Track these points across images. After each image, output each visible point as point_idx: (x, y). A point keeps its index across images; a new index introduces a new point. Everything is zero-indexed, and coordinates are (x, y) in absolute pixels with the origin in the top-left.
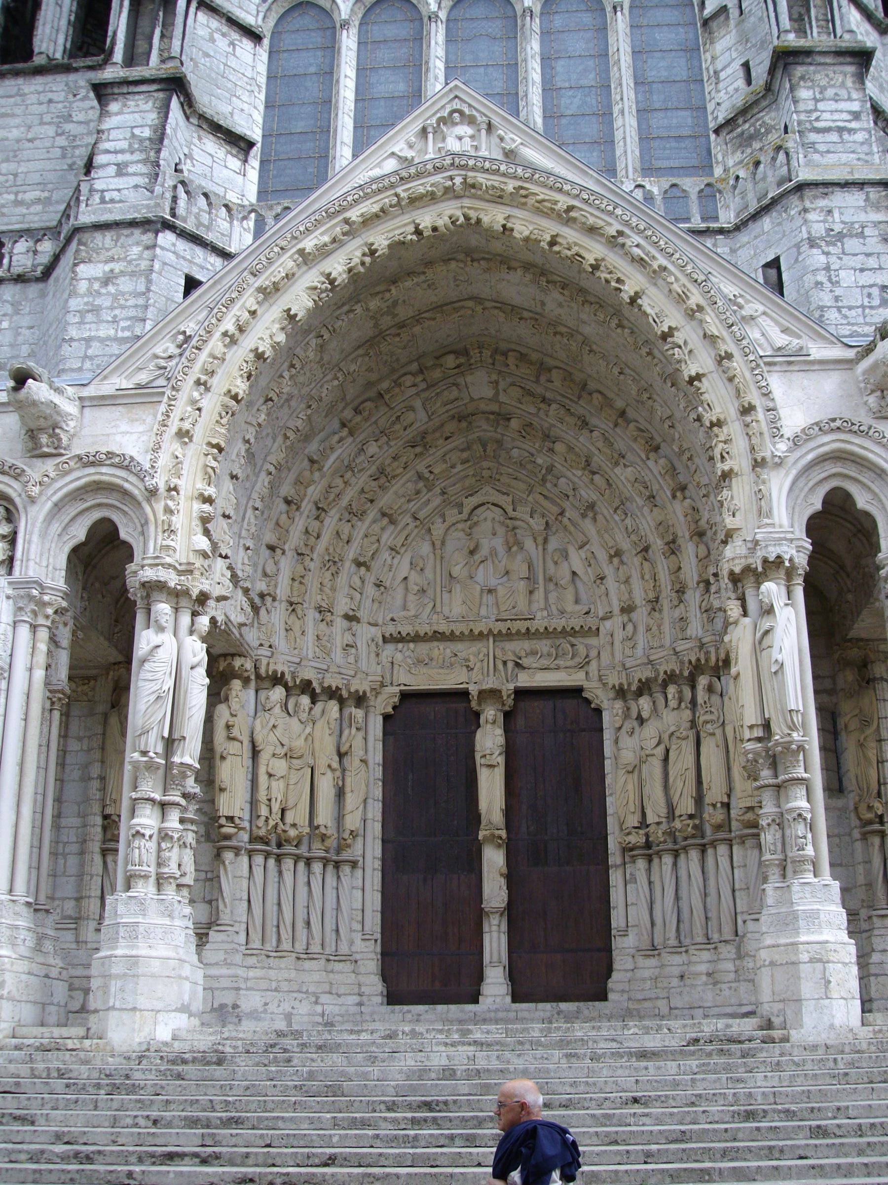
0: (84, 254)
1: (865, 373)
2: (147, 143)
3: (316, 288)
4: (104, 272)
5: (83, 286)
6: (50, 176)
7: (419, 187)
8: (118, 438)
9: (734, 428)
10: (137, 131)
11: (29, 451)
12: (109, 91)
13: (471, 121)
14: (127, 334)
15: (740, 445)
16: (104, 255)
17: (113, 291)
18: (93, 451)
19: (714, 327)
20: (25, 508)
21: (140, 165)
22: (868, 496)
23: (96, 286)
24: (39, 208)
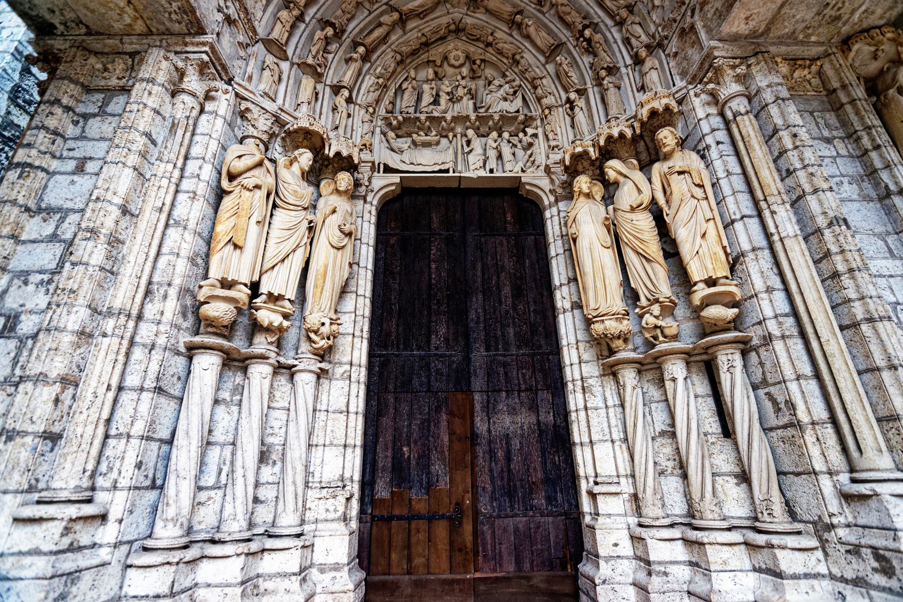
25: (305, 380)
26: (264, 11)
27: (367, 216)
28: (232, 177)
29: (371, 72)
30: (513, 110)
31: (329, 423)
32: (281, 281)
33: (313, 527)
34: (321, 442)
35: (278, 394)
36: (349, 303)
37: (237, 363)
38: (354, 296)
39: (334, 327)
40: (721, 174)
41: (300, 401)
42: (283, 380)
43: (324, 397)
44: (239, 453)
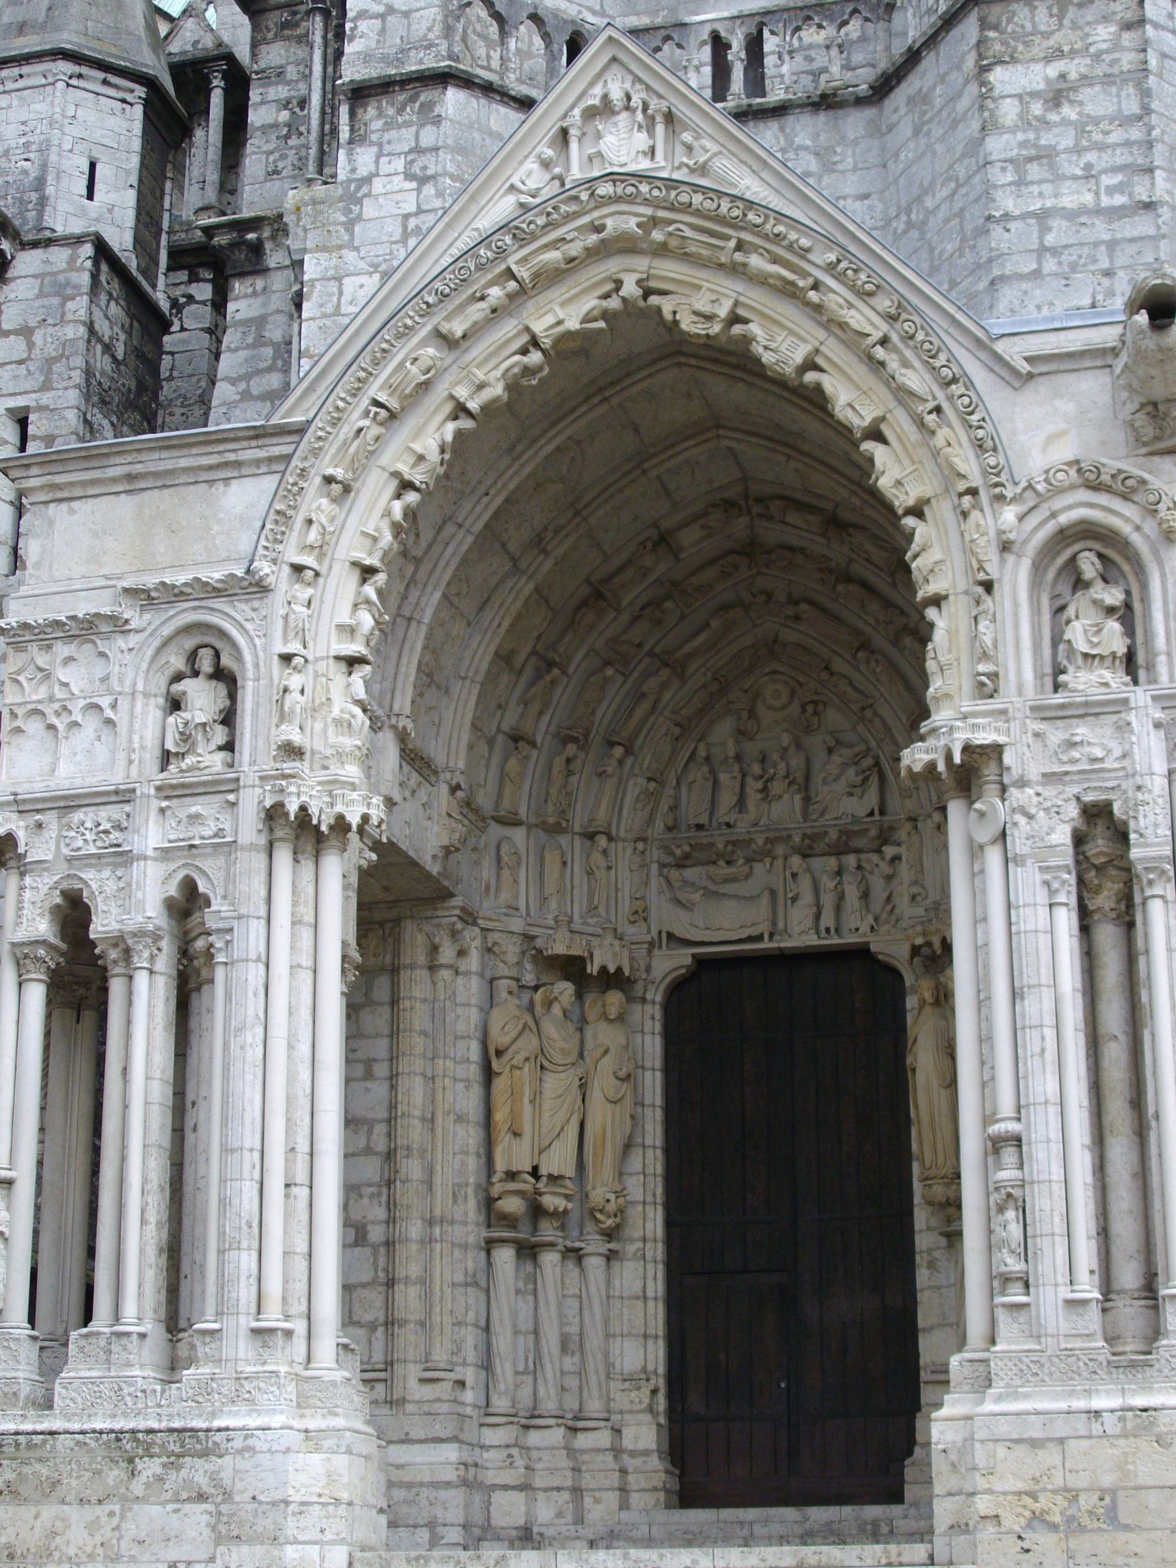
0: (997, 47)
4: (1048, 81)
5: (1009, 111)
11: (1144, 444)
14: (1119, 200)
16: (1040, 47)
17: (1073, 116)
20: (1155, 552)
23: (1037, 108)
25: (595, 1264)
26: (487, 766)
27: (648, 1024)
28: (499, 1053)
29: (636, 771)
30: (862, 811)
31: (625, 1311)
32: (559, 1160)
33: (619, 1417)
34: (618, 1331)
35: (567, 1281)
36: (635, 1162)
37: (528, 1251)
38: (640, 1151)
39: (621, 1200)
41: (593, 1288)
42: (571, 1265)
43: (617, 1283)
44: (543, 1341)
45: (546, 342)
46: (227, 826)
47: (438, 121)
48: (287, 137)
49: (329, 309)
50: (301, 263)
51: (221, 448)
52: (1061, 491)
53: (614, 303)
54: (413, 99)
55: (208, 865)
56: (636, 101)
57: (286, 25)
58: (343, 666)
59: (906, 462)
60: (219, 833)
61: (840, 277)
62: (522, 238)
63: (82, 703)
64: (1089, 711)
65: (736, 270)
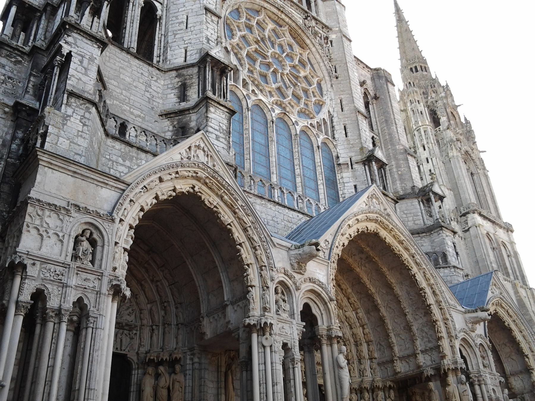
1: (469, 317)
2: (225, 132)
3: (348, 238)
6: (144, 108)
7: (371, 215)
8: (317, 274)
9: (441, 323)
10: (221, 125)
12: (210, 101)
13: (377, 198)
15: (443, 329)
18: (314, 277)
19: (437, 292)
21: (224, 140)
22: (466, 352)
24: (140, 120)
40: (187, 385)
45: (177, 192)
46: (97, 285)
47: (90, 113)
48: (2, 83)
49: (54, 142)
50: (48, 127)
51: (105, 178)
52: (281, 273)
53: (192, 191)
54: (85, 104)
55: (89, 295)
56: (206, 149)
57: (7, 56)
58: (123, 250)
59: (247, 254)
60: (94, 287)
61: (244, 210)
62: (182, 166)
63: (53, 231)
64: (285, 321)
65: (222, 198)
